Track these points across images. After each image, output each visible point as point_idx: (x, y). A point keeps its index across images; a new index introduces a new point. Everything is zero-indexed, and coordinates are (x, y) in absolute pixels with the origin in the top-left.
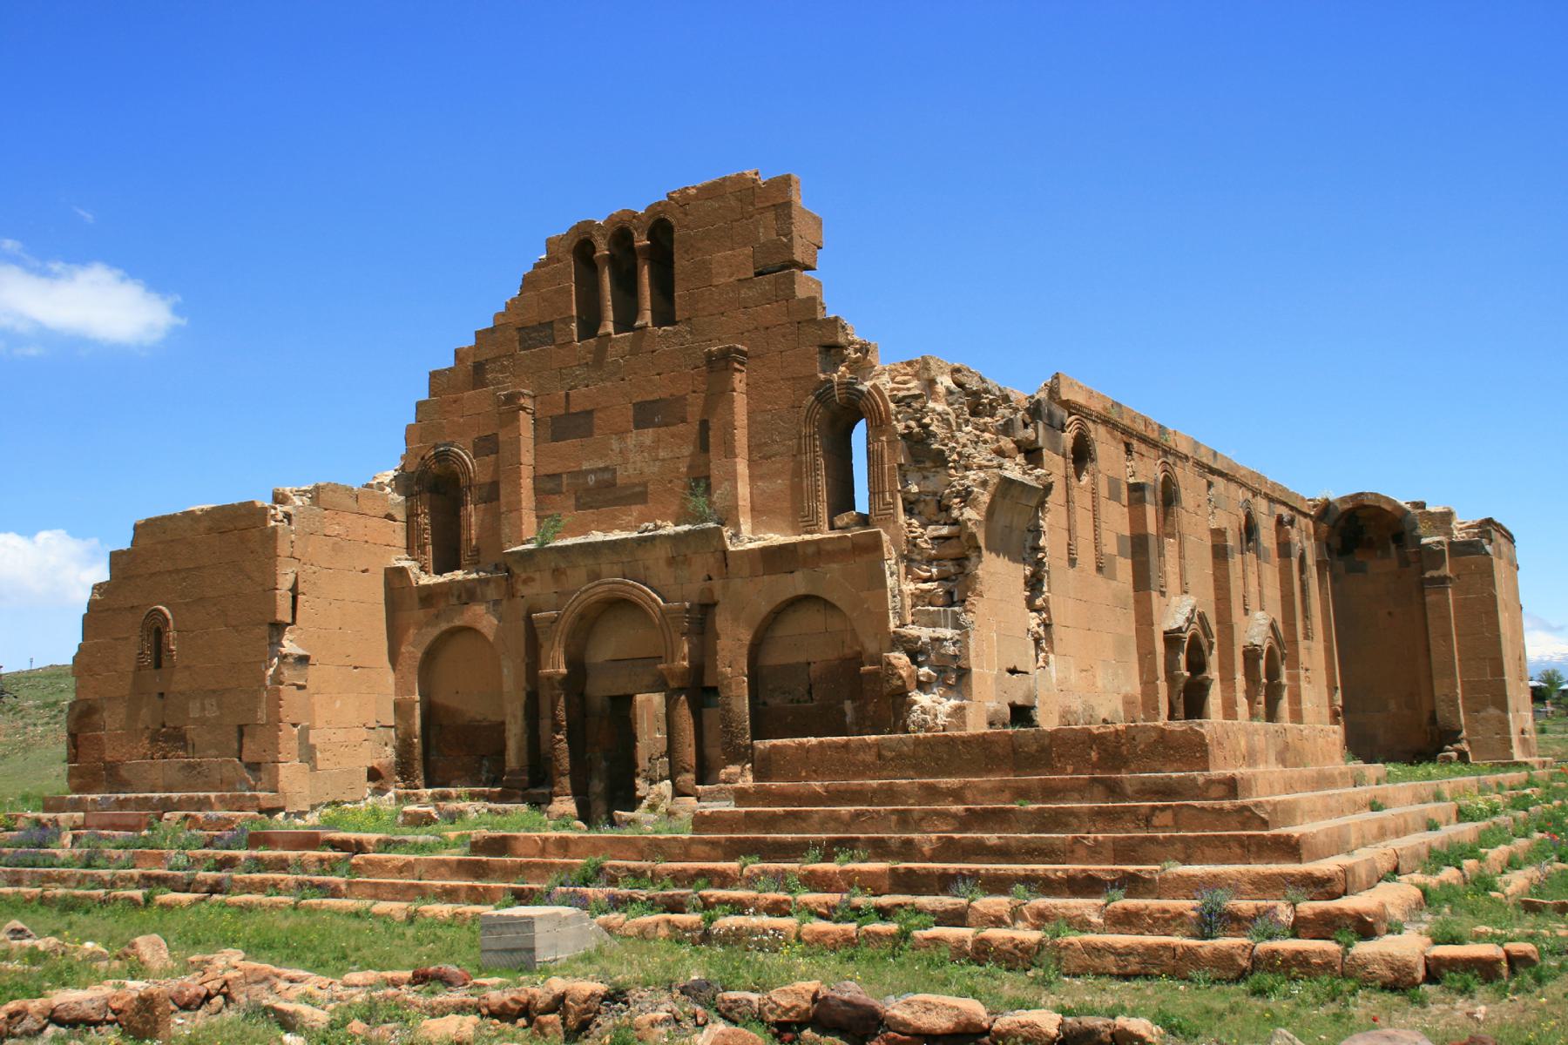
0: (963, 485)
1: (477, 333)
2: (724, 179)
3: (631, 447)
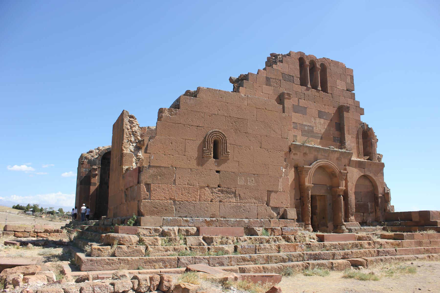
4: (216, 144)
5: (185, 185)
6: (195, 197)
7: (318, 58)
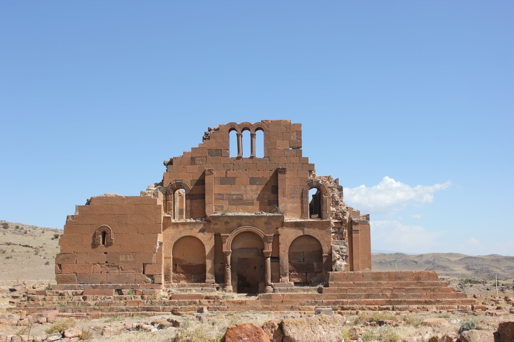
0: (342, 210)
1: (193, 149)
2: (281, 121)
3: (249, 189)
4: (104, 234)
5: (83, 263)
6: (90, 271)
7: (252, 123)
